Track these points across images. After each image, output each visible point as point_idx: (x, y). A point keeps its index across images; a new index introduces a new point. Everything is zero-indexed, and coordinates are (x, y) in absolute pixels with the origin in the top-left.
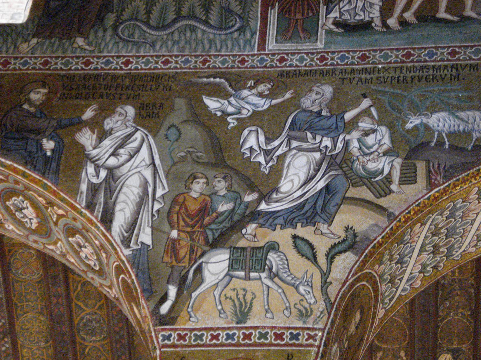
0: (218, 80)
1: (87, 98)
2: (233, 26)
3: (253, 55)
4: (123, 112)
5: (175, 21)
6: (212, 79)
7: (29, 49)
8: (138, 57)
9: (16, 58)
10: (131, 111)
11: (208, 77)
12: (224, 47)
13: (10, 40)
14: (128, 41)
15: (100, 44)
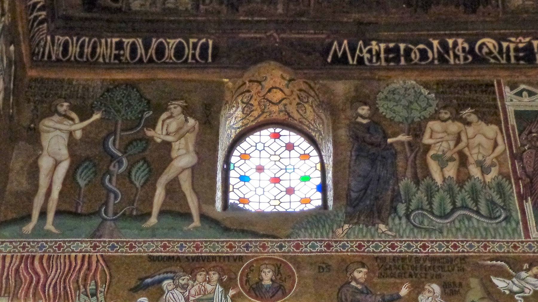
0: (499, 262)
1: (400, 276)
2: (500, 216)
3: (522, 242)
4: (431, 289)
5: (453, 211)
6: (494, 262)
7: (344, 233)
8: (432, 242)
9: (336, 242)
10: (436, 288)
11: (491, 260)
12: (497, 235)
13: (327, 226)
14: (420, 228)
15: (399, 231)
